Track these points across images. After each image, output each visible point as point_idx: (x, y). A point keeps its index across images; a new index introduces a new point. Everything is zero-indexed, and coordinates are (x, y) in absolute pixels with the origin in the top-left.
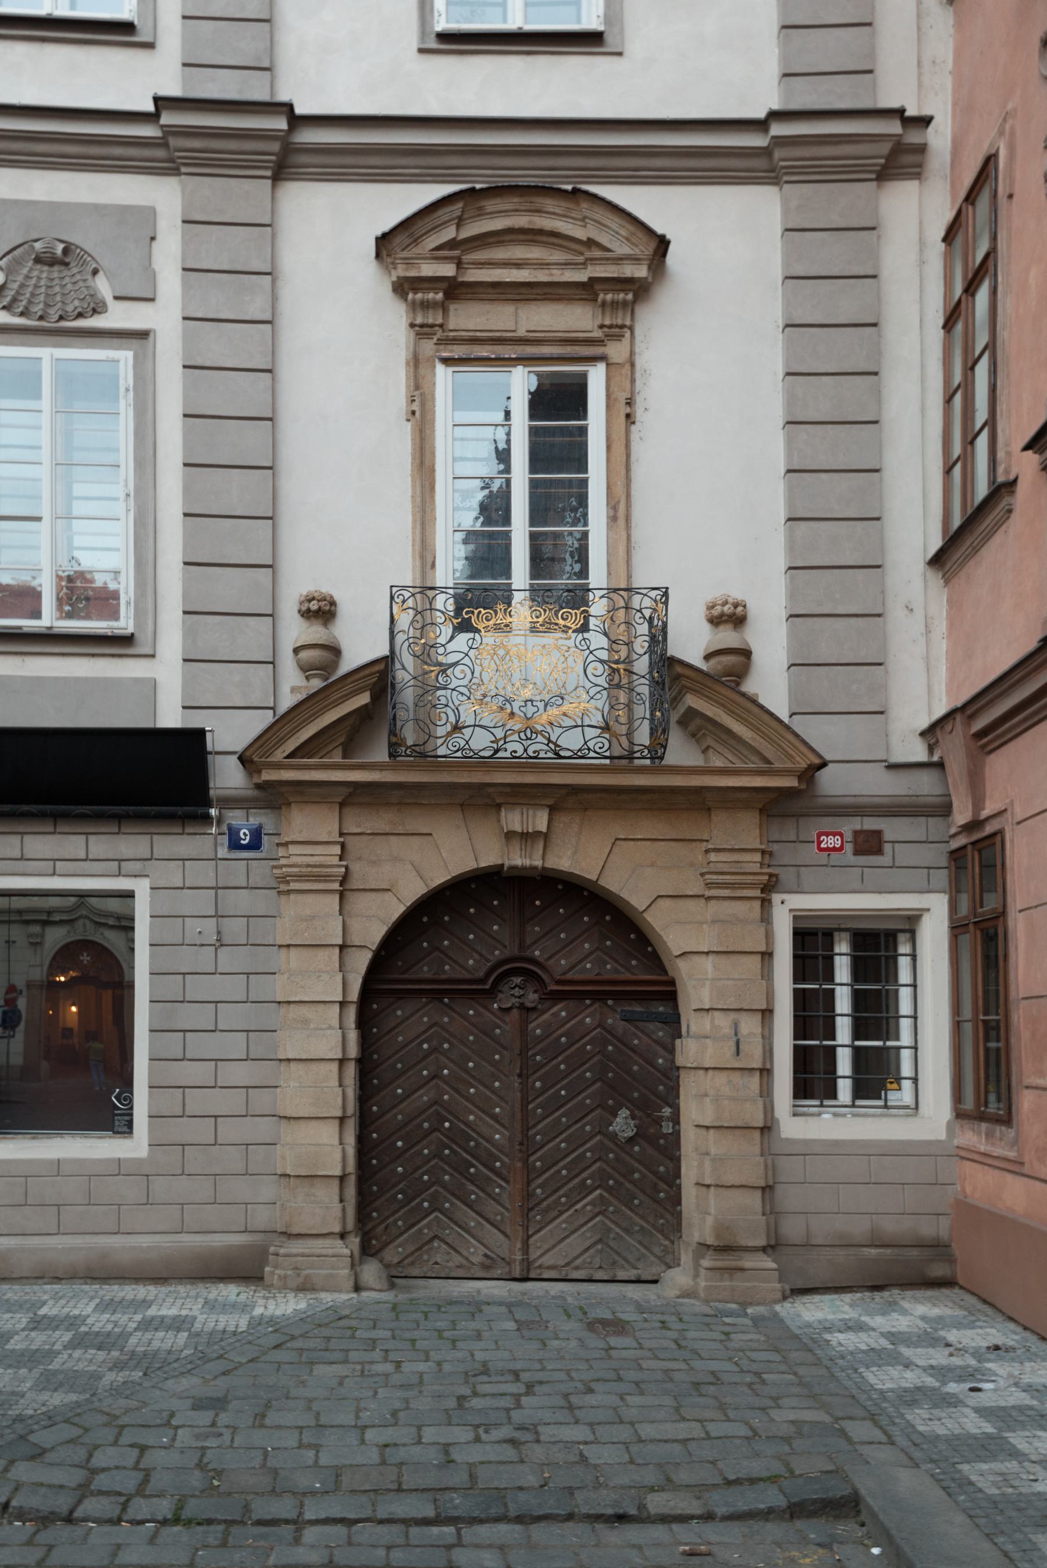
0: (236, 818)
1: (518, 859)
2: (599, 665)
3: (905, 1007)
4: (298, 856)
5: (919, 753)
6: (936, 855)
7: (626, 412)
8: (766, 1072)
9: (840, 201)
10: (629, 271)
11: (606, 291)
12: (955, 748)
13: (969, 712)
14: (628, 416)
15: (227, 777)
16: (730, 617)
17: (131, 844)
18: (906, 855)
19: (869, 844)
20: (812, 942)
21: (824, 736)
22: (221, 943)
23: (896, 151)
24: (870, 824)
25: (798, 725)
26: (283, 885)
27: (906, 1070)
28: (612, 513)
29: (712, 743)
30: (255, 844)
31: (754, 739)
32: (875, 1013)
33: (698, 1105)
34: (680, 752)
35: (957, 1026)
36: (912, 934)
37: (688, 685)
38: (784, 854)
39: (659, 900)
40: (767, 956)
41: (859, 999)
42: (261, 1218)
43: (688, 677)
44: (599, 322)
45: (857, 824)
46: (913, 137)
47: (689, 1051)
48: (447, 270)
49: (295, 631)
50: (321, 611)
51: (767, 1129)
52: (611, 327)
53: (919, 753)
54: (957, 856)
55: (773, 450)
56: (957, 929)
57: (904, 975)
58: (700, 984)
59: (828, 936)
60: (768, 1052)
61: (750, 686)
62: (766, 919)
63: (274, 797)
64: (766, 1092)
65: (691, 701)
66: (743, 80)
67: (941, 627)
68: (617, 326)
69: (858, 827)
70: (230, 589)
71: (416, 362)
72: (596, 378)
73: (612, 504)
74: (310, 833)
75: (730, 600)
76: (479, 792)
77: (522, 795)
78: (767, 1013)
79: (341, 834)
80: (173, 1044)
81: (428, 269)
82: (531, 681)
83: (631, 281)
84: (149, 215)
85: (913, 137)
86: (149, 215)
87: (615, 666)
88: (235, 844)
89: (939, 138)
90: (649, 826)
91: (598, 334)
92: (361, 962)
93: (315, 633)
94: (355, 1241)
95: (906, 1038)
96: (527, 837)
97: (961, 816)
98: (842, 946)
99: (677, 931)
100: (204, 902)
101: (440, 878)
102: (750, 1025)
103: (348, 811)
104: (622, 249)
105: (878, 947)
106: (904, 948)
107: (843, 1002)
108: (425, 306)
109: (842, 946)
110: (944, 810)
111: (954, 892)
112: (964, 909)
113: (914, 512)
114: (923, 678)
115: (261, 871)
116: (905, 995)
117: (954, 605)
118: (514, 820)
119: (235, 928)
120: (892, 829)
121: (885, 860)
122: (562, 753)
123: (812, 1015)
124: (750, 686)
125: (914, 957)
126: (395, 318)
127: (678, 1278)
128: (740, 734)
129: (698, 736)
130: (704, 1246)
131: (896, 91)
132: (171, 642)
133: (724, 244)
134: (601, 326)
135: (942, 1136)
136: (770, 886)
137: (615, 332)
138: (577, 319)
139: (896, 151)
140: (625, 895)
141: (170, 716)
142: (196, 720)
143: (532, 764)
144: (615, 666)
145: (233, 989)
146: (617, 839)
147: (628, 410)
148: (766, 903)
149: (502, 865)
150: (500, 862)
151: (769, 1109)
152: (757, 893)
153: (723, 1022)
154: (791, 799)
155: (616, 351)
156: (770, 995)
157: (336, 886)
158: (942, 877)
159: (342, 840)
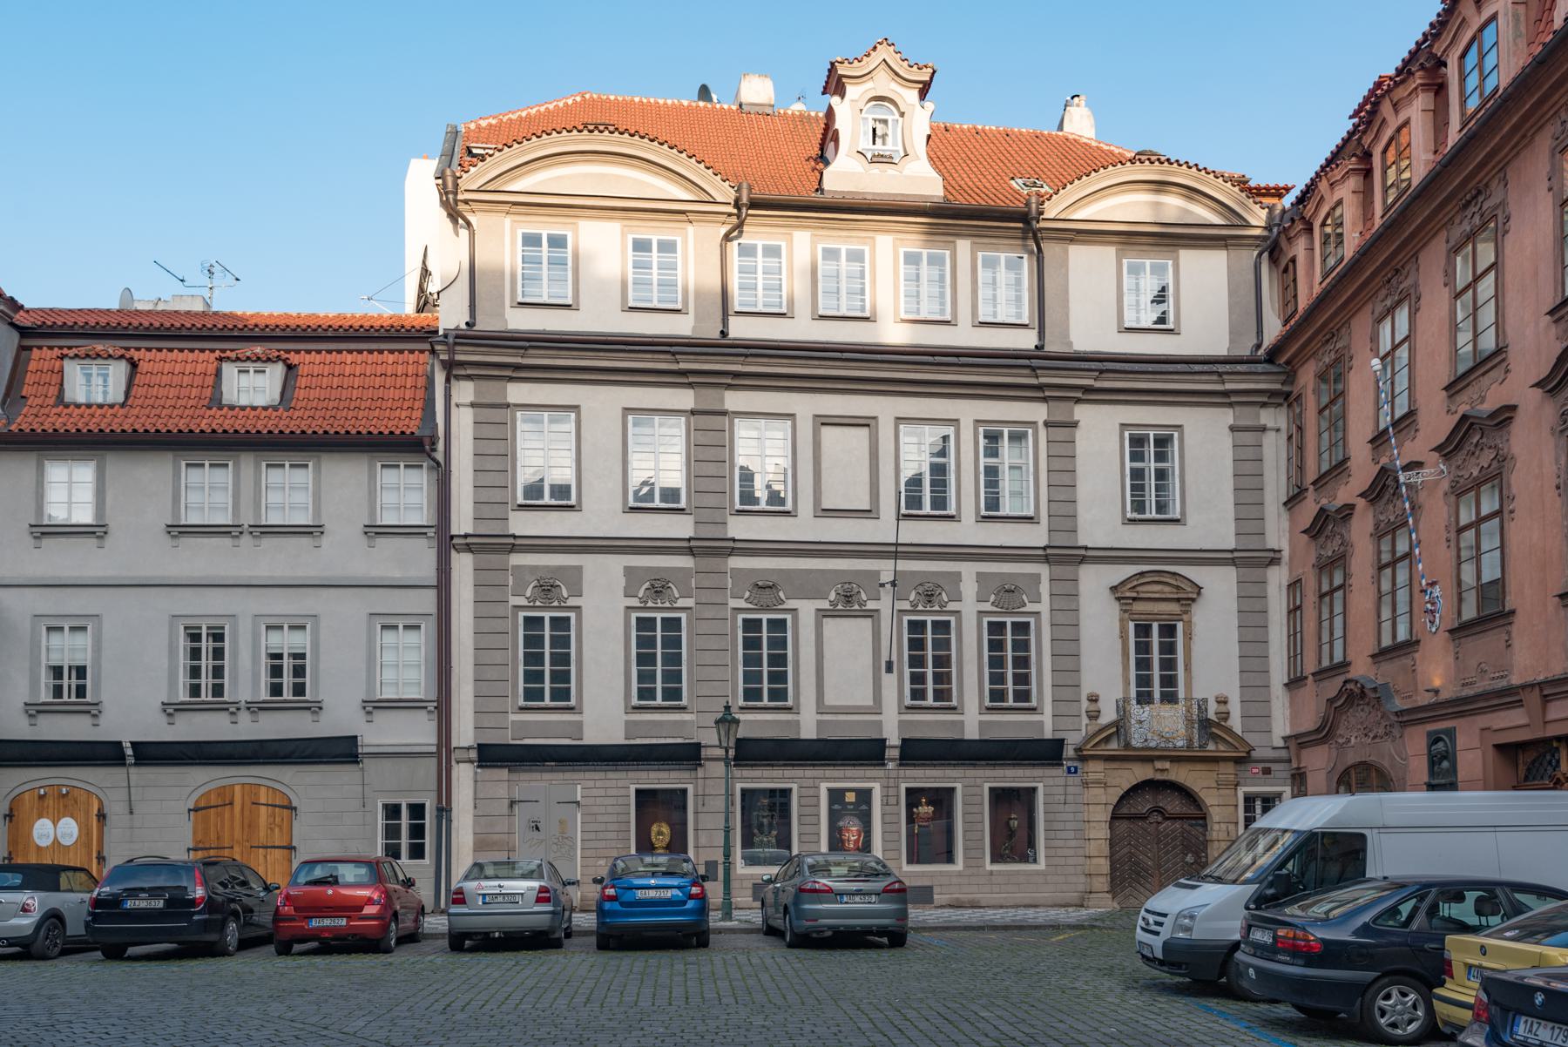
0: (1070, 764)
1: (1159, 777)
4: (1092, 776)
6: (1287, 775)
7: (1188, 636)
9: (1253, 573)
15: (1069, 752)
16: (1222, 701)
17: (1038, 772)
18: (1278, 774)
19: (1267, 771)
21: (1252, 739)
23: (1273, 559)
26: (1086, 784)
38: (1241, 774)
42: (1081, 888)
53: (1281, 744)
54: (1293, 776)
58: (1216, 814)
61: (1229, 723)
63: (1083, 759)
66: (1224, 536)
70: (1067, 693)
71: (1121, 620)
72: (1180, 626)
74: (1095, 769)
76: (1146, 757)
77: (1160, 758)
82: (1163, 724)
83: (1189, 596)
84: (1038, 576)
86: (1038, 576)
89: (1286, 554)
90: (1199, 766)
93: (1093, 707)
97: (1295, 765)
99: (1210, 798)
110: (1289, 761)
111: (1293, 785)
113: (1279, 672)
118: (1159, 765)
120: (1274, 767)
124: (1229, 723)
126: (1115, 607)
131: (1272, 542)
133: (1219, 585)
137: (1186, 612)
138: (1174, 608)
139: (1274, 559)
141: (1048, 734)
142: (1059, 736)
145: (1071, 817)
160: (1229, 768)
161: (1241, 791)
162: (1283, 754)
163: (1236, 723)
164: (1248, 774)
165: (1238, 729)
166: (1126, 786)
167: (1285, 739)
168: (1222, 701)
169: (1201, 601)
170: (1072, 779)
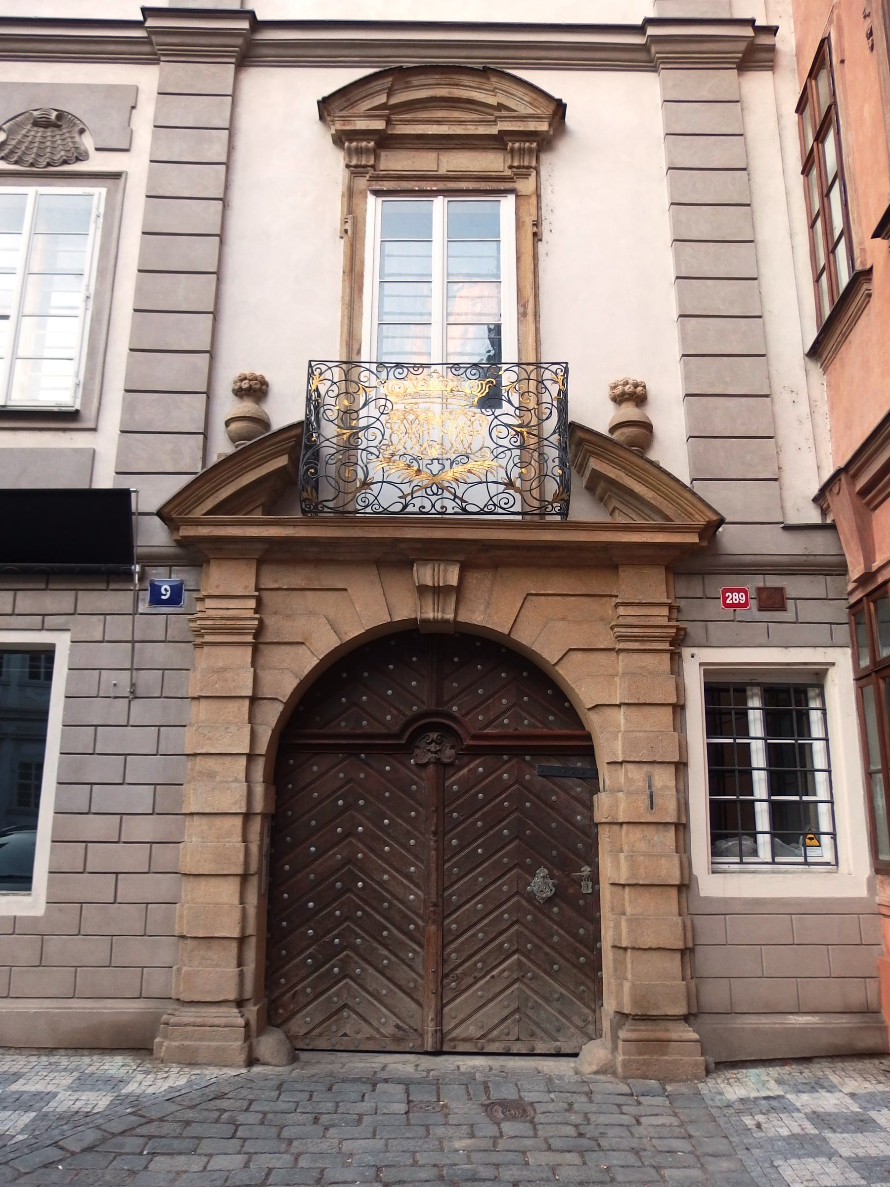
2: (504, 429)
3: (819, 761)
5: (813, 516)
6: (839, 611)
8: (682, 827)
10: (532, 126)
11: (514, 142)
12: (843, 509)
13: (852, 472)
14: (535, 234)
15: (152, 535)
17: (56, 600)
18: (808, 611)
19: (773, 600)
20: (724, 698)
21: (722, 498)
22: (134, 695)
24: (773, 581)
25: (698, 487)
26: (200, 638)
27: (825, 825)
28: (522, 310)
29: (618, 505)
30: (175, 599)
31: (655, 499)
32: (792, 769)
33: (614, 863)
34: (583, 509)
35: (869, 775)
36: (821, 687)
37: (591, 449)
38: (691, 610)
39: (571, 653)
40: (679, 708)
41: (773, 753)
42: (156, 983)
43: (589, 442)
44: (509, 163)
45: (759, 581)
46: (764, 40)
47: (605, 806)
48: (379, 125)
49: (228, 405)
50: (254, 389)
51: (685, 886)
52: (518, 167)
55: (665, 263)
56: (861, 678)
57: (816, 730)
59: (741, 691)
60: (683, 806)
62: (676, 669)
63: (195, 554)
64: (683, 847)
65: (594, 464)
67: (823, 408)
68: (524, 167)
69: (761, 585)
73: (522, 302)
74: (228, 587)
75: (631, 382)
76: (393, 547)
78: (681, 766)
79: (257, 589)
80: (79, 797)
81: (361, 125)
85: (764, 40)
87: (518, 429)
88: (156, 599)
90: (558, 583)
91: (508, 173)
92: (271, 715)
94: (252, 1010)
95: (822, 793)
96: (439, 592)
97: (856, 571)
98: (755, 702)
100: (120, 655)
101: (353, 631)
102: (664, 778)
103: (266, 570)
104: (524, 109)
105: (791, 700)
106: (814, 704)
107: (758, 758)
108: (359, 152)
109: (755, 702)
112: (865, 662)
113: (791, 311)
114: (811, 447)
115: (179, 625)
116: (818, 747)
117: (833, 388)
118: (426, 575)
119: (148, 680)
120: (794, 586)
121: (789, 615)
122: (470, 508)
123: (727, 770)
125: (824, 710)
127: (595, 1054)
128: (641, 494)
129: (608, 508)
130: (622, 1016)
132: (112, 419)
134: (511, 167)
135: (862, 892)
136: (678, 642)
137: (522, 172)
140: (536, 648)
141: (105, 479)
143: (442, 521)
144: (518, 429)
145: (143, 740)
146: (528, 595)
147: (535, 229)
148: (676, 657)
149: (416, 619)
150: (413, 616)
151: (686, 866)
152: (666, 646)
153: (637, 774)
154: (695, 556)
155: (526, 186)
156: (683, 747)
157: (250, 639)
158: (843, 633)
159: (257, 594)
160: (651, 586)
161: (695, 664)
162: (819, 546)
163: (673, 453)
164: (715, 609)
165: (682, 473)
166: (326, 643)
167: (820, 499)
168: (635, 396)
169: (564, 149)
170: (155, 623)
